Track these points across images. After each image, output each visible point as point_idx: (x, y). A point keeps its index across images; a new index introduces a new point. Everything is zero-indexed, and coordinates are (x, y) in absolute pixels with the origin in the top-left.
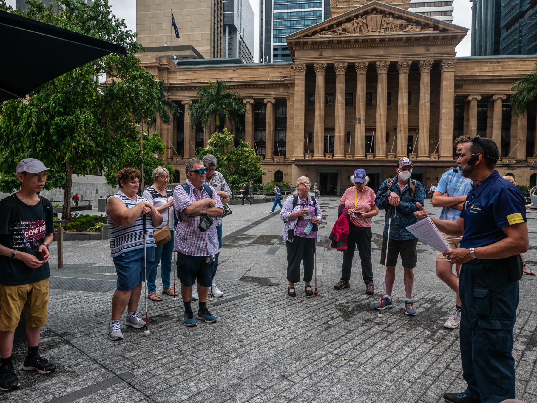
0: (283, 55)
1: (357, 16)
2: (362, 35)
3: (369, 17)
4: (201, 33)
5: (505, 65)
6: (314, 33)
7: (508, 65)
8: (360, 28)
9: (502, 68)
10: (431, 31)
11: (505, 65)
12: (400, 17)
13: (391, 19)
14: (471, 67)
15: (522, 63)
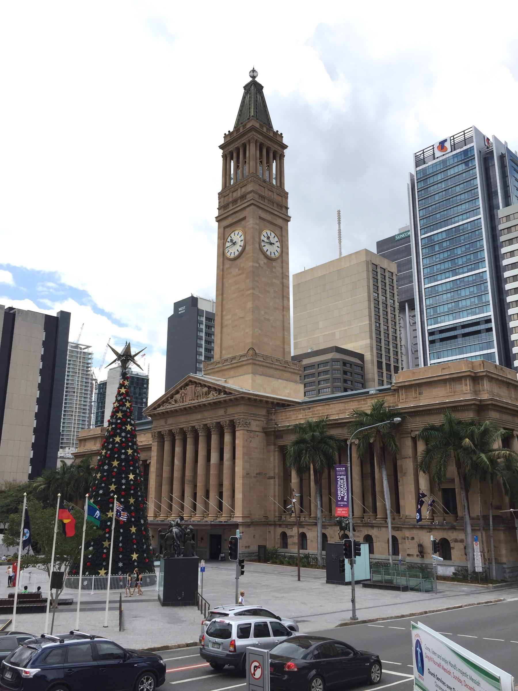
0: (442, 340)
1: (181, 388)
2: (185, 404)
3: (187, 387)
4: (359, 325)
5: (314, 411)
6: (159, 406)
7: (317, 410)
8: (183, 398)
9: (313, 414)
10: (223, 395)
11: (314, 411)
12: (205, 386)
13: (200, 388)
14: (289, 415)
15: (327, 407)
